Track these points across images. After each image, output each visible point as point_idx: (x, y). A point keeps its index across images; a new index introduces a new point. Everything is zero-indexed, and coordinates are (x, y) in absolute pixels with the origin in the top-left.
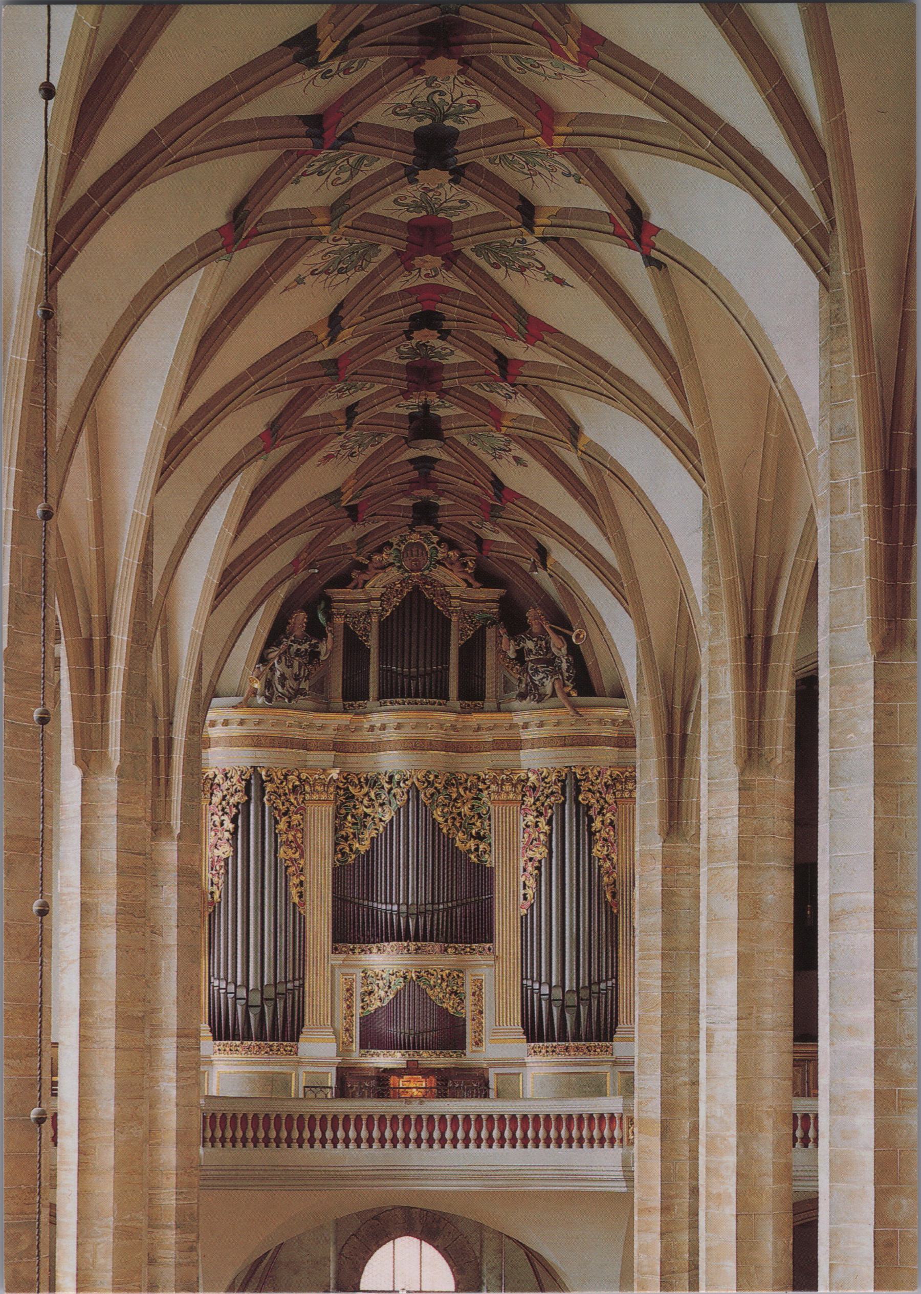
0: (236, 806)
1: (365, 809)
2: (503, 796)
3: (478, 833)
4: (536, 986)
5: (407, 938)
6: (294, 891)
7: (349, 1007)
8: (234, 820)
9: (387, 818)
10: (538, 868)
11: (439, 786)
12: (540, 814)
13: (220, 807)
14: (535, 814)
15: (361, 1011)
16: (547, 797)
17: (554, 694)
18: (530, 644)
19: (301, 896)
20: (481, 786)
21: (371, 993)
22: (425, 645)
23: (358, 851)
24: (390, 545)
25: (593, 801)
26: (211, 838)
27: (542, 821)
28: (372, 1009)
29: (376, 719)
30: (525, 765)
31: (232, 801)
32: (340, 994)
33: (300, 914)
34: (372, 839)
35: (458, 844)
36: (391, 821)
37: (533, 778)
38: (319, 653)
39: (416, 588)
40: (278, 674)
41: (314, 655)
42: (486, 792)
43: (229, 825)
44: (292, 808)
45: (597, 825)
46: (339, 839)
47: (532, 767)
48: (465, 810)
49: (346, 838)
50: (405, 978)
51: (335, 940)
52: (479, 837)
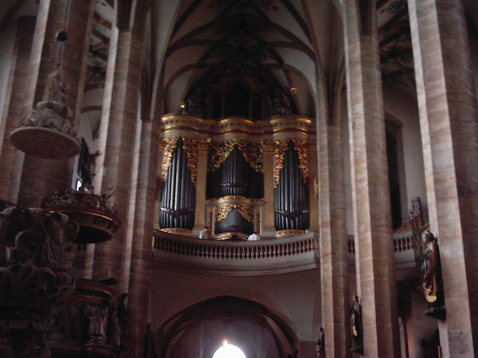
0: (173, 149)
1: (219, 154)
2: (268, 149)
3: (259, 162)
4: (280, 211)
6: (192, 178)
7: (211, 219)
9: (226, 156)
10: (280, 172)
11: (245, 145)
12: (280, 154)
14: (279, 154)
15: (216, 221)
16: (283, 148)
17: (285, 114)
18: (277, 100)
19: (195, 180)
20: (260, 147)
21: (220, 214)
23: (216, 167)
25: (299, 149)
26: (164, 161)
27: (282, 156)
28: (219, 220)
29: (222, 121)
30: (275, 139)
32: (208, 215)
35: (252, 166)
37: (278, 143)
40: (190, 105)
42: (261, 149)
43: (171, 156)
44: (193, 151)
45: (300, 158)
46: (210, 164)
47: (278, 139)
48: (255, 155)
50: (232, 207)
52: (259, 164)
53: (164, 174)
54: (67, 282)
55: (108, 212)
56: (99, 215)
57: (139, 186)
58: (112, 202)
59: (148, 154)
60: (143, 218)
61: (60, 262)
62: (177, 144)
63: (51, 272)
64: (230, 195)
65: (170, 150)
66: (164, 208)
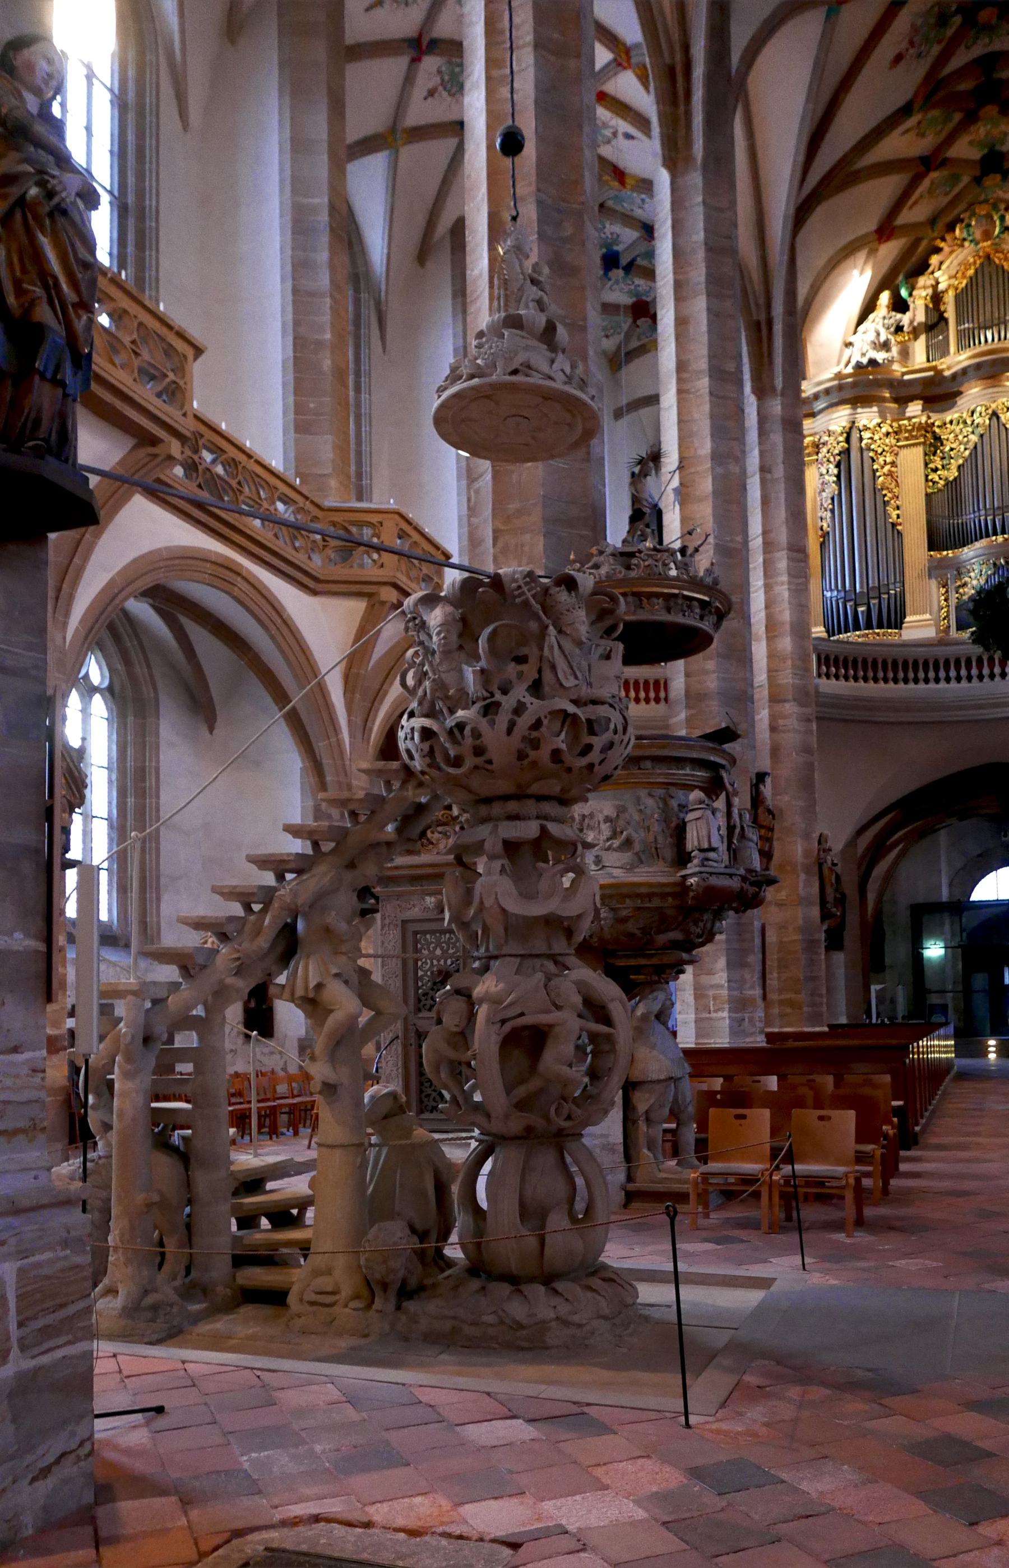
0: (839, 455)
5: (995, 534)
6: (894, 514)
8: (838, 466)
9: (971, 446)
13: (825, 460)
22: (998, 286)
24: (962, 221)
31: (837, 451)
33: (899, 532)
34: (959, 467)
36: (975, 447)
38: (903, 327)
39: (988, 257)
41: (899, 329)
49: (935, 470)
50: (995, 564)
51: (930, 550)
53: (824, 515)
54: (612, 726)
55: (696, 583)
56: (676, 591)
57: (768, 546)
58: (702, 562)
59: (779, 471)
60: (786, 615)
61: (590, 684)
62: (848, 440)
63: (571, 709)
64: (988, 536)
65: (832, 459)
66: (831, 590)
